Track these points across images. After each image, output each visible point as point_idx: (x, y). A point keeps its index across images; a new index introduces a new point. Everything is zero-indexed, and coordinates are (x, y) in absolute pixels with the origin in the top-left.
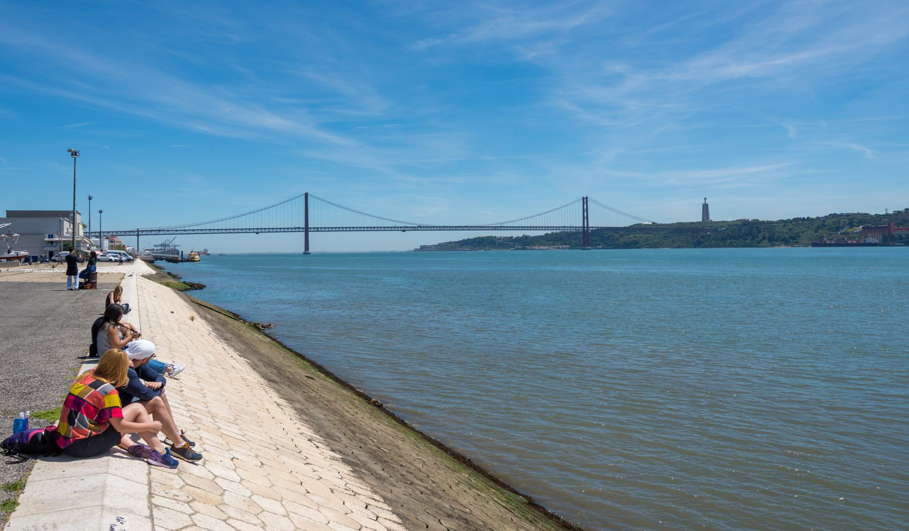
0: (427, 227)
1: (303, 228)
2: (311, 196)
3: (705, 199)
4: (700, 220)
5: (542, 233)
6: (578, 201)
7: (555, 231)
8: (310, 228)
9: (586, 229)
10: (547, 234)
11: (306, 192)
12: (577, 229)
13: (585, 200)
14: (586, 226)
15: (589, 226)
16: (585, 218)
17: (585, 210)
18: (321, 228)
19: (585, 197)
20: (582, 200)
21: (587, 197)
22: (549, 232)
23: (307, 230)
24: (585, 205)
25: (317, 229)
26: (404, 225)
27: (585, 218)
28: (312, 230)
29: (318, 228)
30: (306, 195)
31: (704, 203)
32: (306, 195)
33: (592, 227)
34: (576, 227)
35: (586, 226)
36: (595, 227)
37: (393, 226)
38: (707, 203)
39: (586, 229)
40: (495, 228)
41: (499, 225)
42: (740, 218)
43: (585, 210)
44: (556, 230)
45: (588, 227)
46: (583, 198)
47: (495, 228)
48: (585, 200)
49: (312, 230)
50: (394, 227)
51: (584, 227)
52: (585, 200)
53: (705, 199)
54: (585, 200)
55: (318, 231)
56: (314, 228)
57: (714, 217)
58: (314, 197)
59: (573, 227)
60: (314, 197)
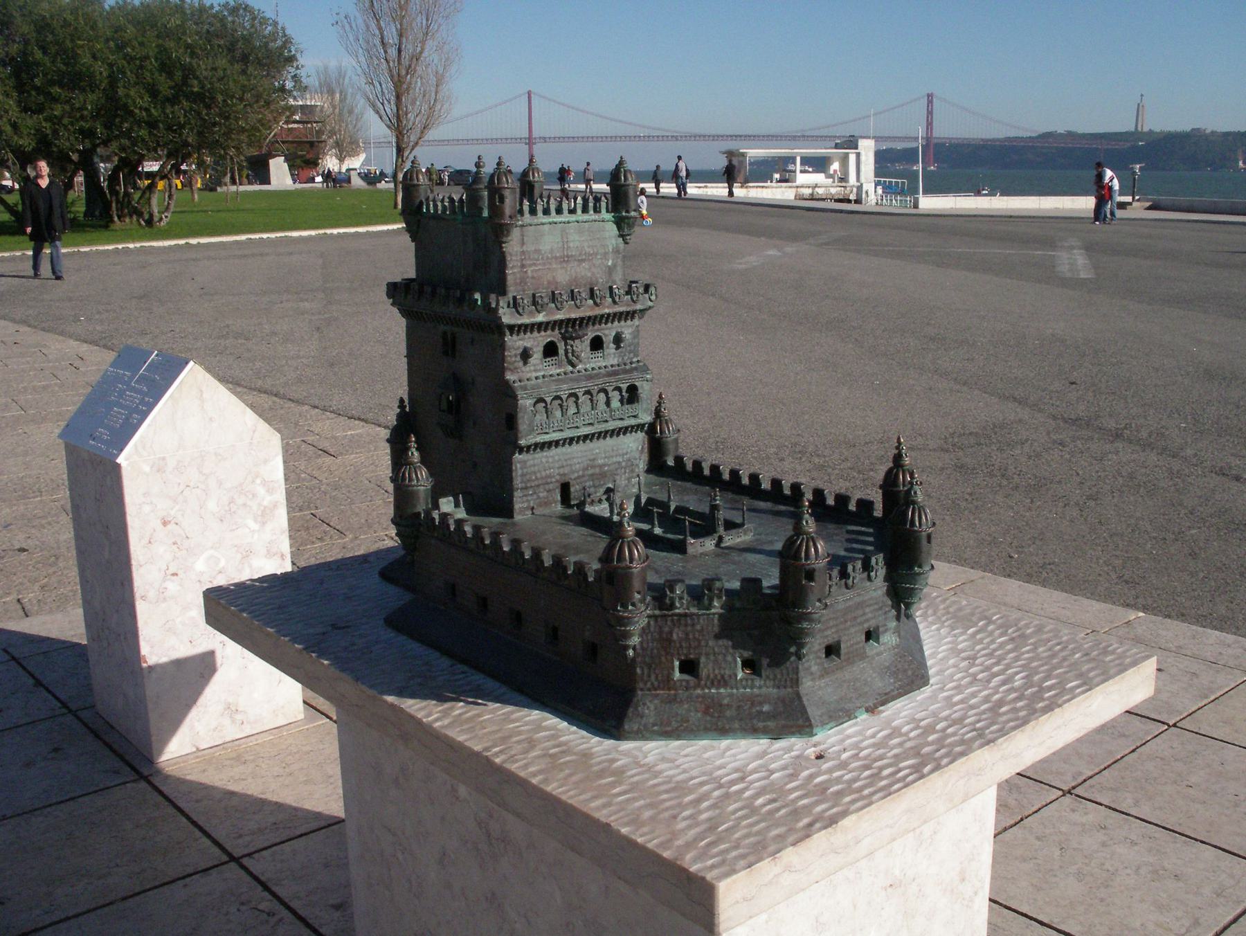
1: (525, 138)
2: (534, 94)
8: (535, 138)
11: (526, 91)
16: (929, 125)
23: (530, 141)
25: (544, 139)
27: (929, 125)
30: (529, 93)
32: (529, 93)
33: (939, 138)
46: (928, 95)
51: (928, 139)
55: (545, 142)
58: (540, 96)
60: (540, 96)
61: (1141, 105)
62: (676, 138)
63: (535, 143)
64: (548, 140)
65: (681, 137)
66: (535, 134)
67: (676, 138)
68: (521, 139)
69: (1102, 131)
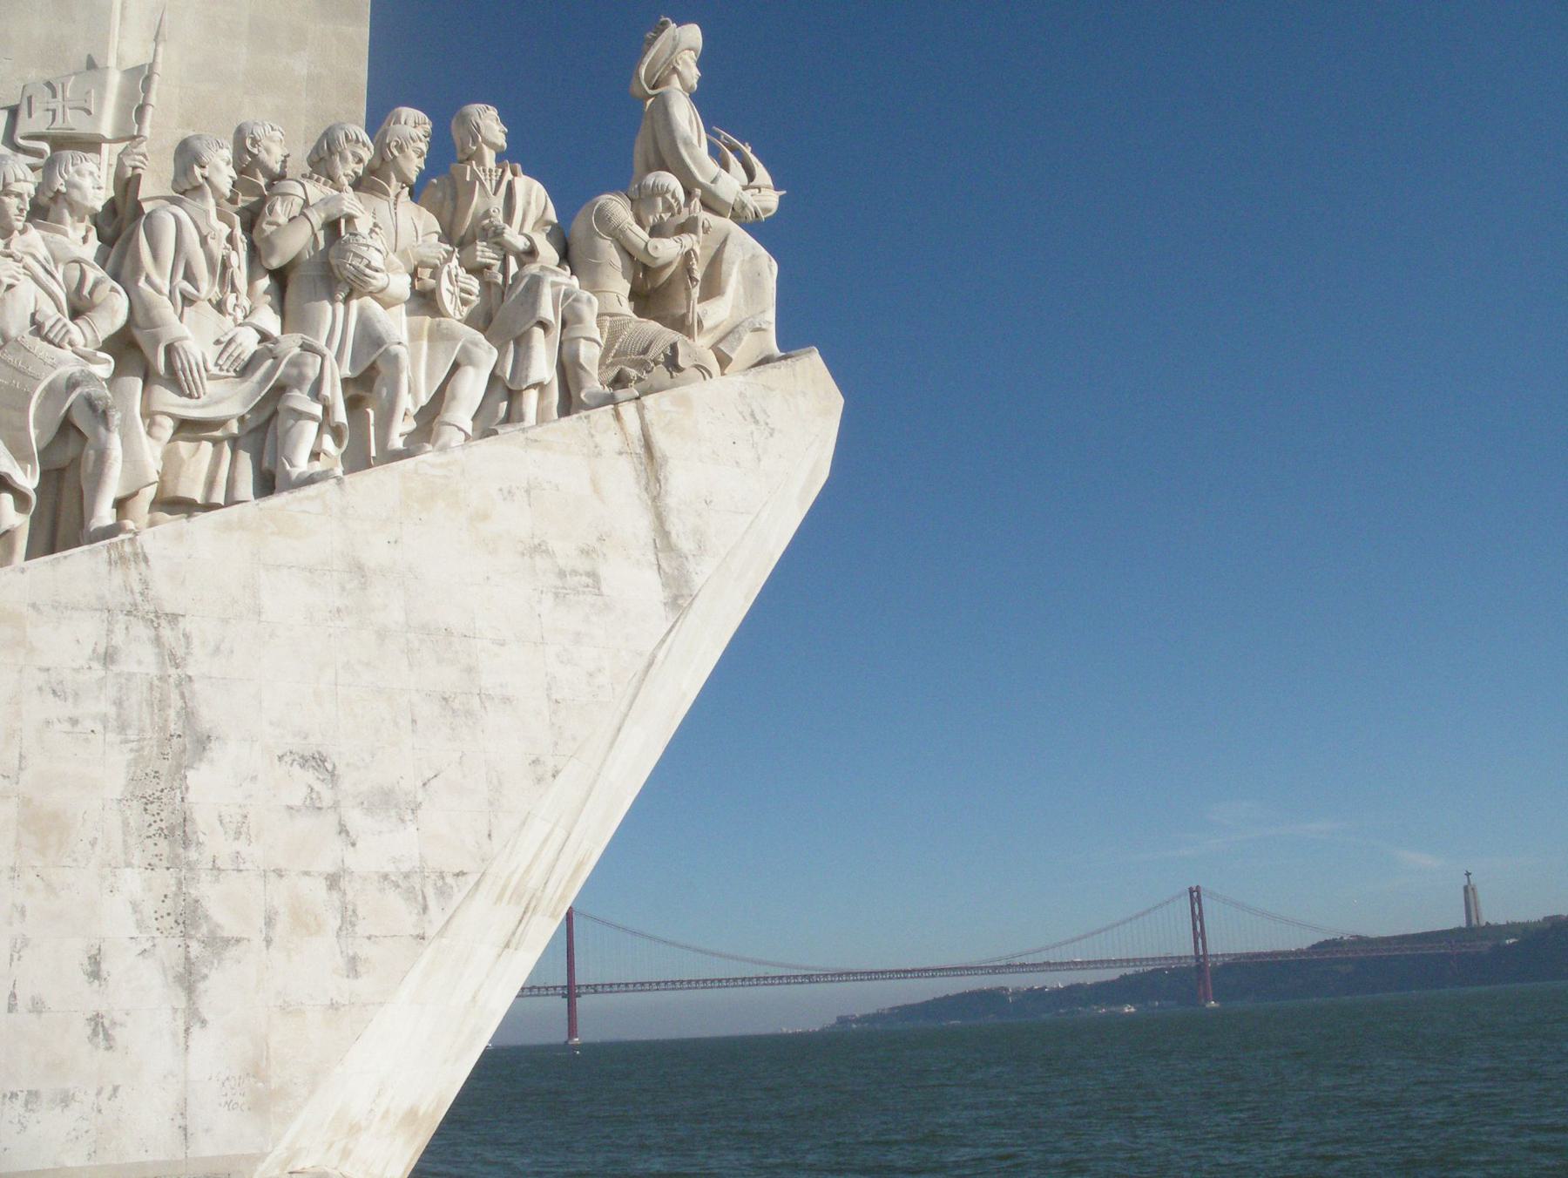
0: (840, 975)
1: (563, 987)
3: (1468, 874)
4: (1461, 922)
5: (1112, 974)
6: (1179, 896)
7: (1141, 969)
8: (579, 987)
9: (1202, 960)
10: (1124, 978)
12: (1183, 961)
13: (1195, 895)
14: (1201, 953)
15: (1209, 953)
16: (1199, 935)
17: (1197, 917)
18: (603, 985)
19: (1194, 886)
20: (1189, 894)
21: (1198, 889)
22: (1129, 971)
23: (571, 992)
24: (1196, 906)
25: (594, 989)
26: (789, 972)
27: (1199, 935)
28: (584, 990)
29: (596, 985)
31: (1466, 883)
33: (1217, 956)
34: (1180, 958)
35: (1201, 953)
36: (1229, 955)
37: (762, 975)
38: (1472, 883)
39: (1202, 960)
40: (996, 970)
41: (1003, 963)
42: (1549, 913)
43: (1197, 917)
44: (1135, 966)
45: (1205, 956)
46: (1191, 891)
47: (996, 970)
48: (1195, 895)
49: (584, 990)
50: (766, 978)
51: (1197, 957)
52: (1195, 894)
53: (1468, 874)
54: (1195, 894)
55: (596, 992)
56: (587, 986)
57: (1493, 913)
59: (1172, 958)
61: (1470, 888)
62: (809, 979)
63: (579, 995)
64: (599, 989)
65: (818, 976)
66: (579, 979)
67: (809, 979)
68: (555, 988)
69: (1420, 930)
